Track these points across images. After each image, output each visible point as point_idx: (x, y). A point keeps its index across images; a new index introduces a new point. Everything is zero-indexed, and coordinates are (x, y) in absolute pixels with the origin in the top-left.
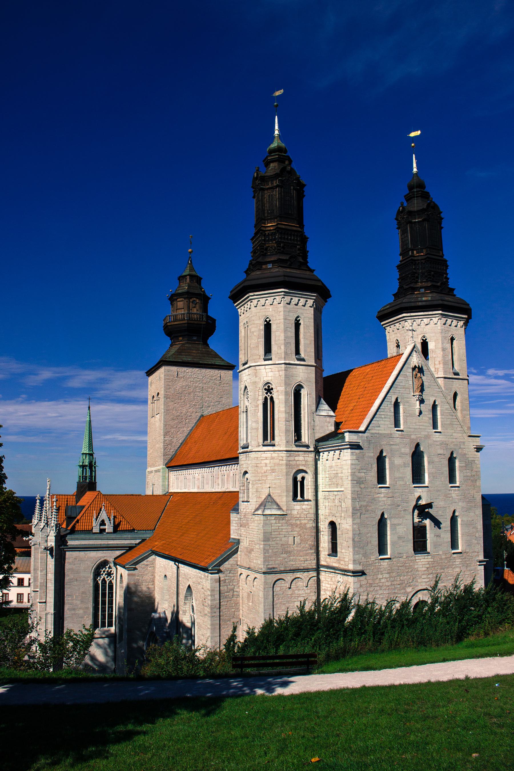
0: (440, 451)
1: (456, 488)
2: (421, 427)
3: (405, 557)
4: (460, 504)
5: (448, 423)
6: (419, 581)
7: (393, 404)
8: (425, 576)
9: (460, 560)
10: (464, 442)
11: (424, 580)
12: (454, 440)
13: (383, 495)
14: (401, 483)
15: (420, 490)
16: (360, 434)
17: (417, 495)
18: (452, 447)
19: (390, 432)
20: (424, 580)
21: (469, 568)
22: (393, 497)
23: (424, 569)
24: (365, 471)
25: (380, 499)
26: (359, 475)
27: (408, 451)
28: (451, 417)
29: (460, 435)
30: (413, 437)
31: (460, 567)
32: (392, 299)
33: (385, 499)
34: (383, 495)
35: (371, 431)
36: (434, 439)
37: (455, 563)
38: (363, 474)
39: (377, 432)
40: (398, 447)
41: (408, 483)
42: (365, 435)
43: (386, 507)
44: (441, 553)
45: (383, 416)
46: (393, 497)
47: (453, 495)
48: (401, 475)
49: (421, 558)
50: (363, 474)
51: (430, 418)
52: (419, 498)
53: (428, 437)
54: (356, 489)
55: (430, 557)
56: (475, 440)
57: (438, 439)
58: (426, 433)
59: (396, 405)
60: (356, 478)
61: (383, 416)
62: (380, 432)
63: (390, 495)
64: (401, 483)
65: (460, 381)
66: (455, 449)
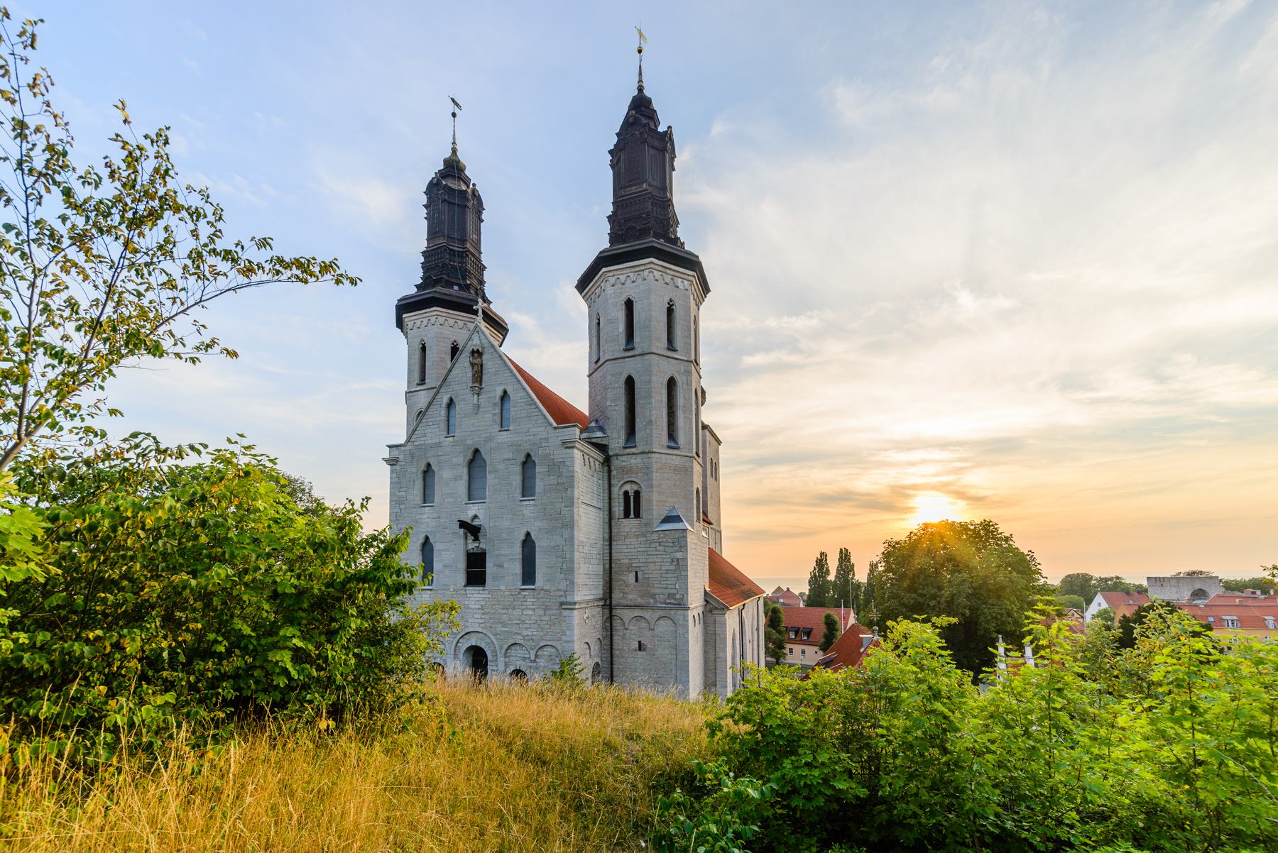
0: (510, 456)
1: (531, 502)
2: (480, 428)
3: (452, 590)
4: (537, 523)
5: (524, 415)
6: (470, 620)
7: (444, 405)
8: (479, 616)
9: (533, 600)
10: (547, 438)
11: (476, 621)
13: (426, 516)
14: (451, 500)
16: (402, 448)
18: (526, 448)
19: (438, 441)
20: (476, 621)
21: (548, 612)
22: (439, 517)
23: (477, 607)
24: (405, 489)
25: (423, 521)
26: (398, 494)
27: (462, 460)
28: (528, 407)
29: (542, 429)
30: (470, 442)
31: (534, 610)
32: (414, 291)
33: (427, 520)
34: (426, 516)
35: (415, 444)
36: (499, 441)
37: (525, 603)
38: (404, 493)
39: (422, 443)
40: (448, 457)
41: (459, 500)
42: (407, 448)
43: (429, 530)
44: (503, 587)
45: (431, 423)
46: (439, 517)
47: (525, 512)
48: (450, 491)
49: (473, 592)
50: (404, 493)
51: (494, 415)
52: (476, 516)
53: (489, 439)
54: (395, 511)
55: (486, 592)
56: (567, 433)
57: (505, 440)
58: (488, 435)
60: (396, 499)
61: (431, 423)
62: (426, 442)
63: (436, 515)
64: (451, 500)
65: (638, 358)
66: (532, 450)
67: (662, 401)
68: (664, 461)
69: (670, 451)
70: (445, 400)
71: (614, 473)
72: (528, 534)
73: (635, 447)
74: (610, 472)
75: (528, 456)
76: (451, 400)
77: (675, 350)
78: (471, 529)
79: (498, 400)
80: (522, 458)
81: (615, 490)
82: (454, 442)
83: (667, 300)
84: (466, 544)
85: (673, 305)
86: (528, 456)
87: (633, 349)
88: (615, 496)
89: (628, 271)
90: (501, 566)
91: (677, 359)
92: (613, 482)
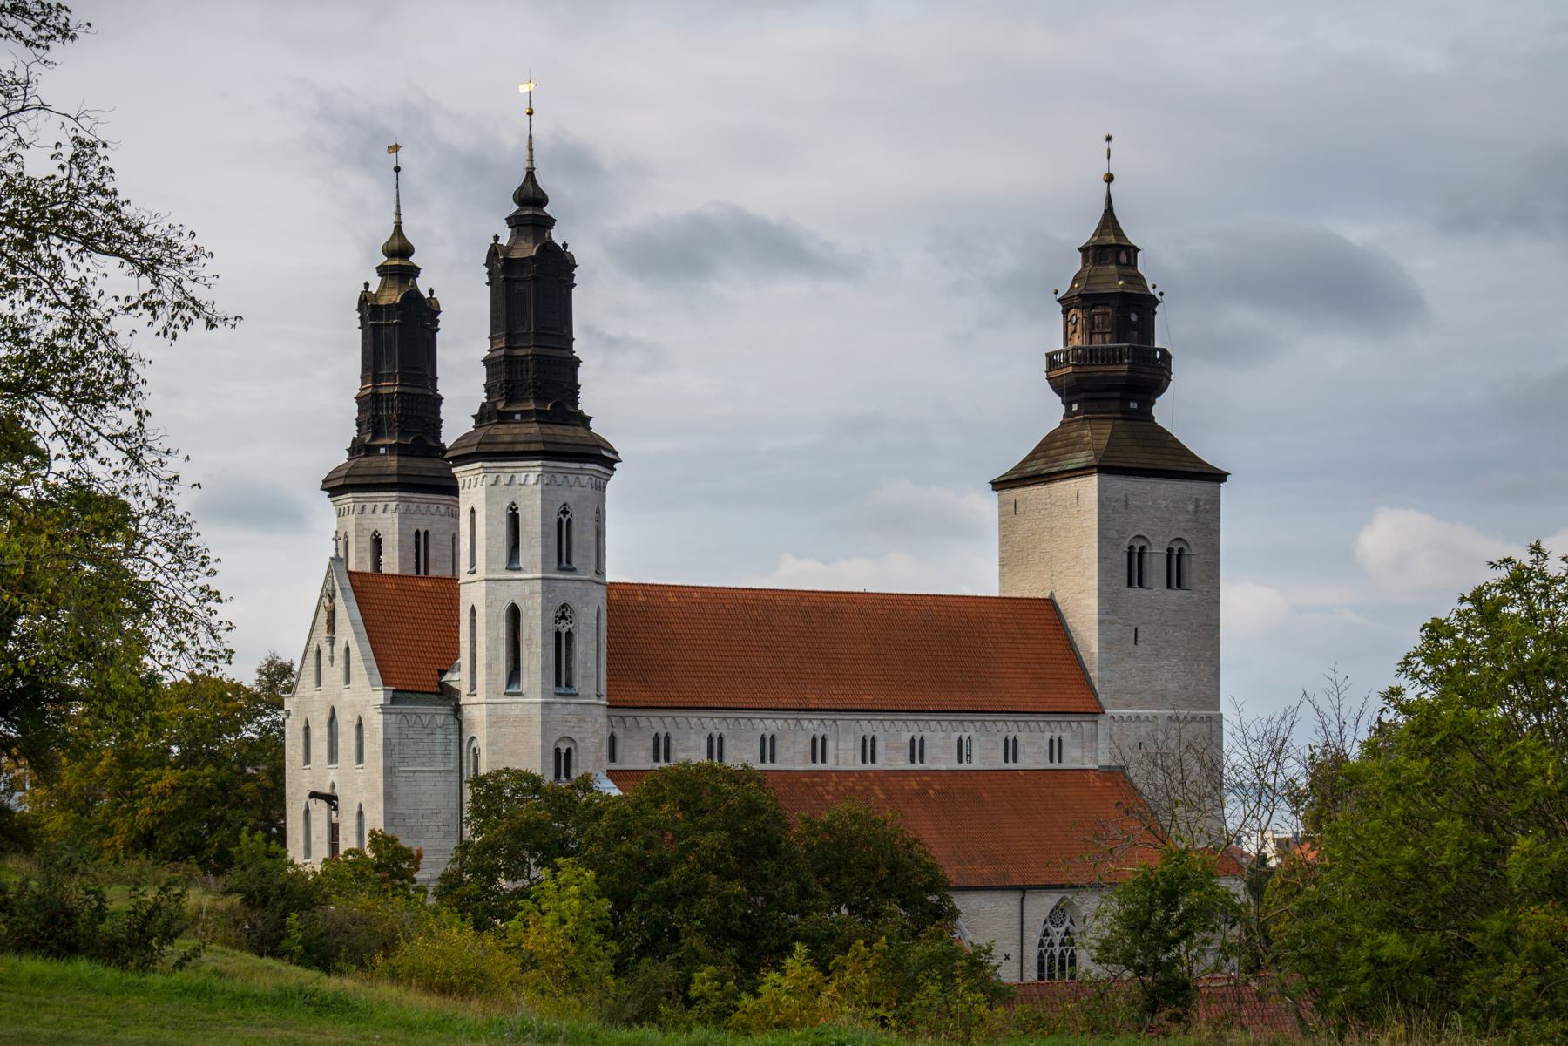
0: (349, 717)
12: (361, 698)
15: (332, 772)
17: (330, 779)
30: (329, 698)
59: (319, 653)
67: (498, 637)
68: (500, 712)
69: (510, 699)
70: (315, 648)
71: (464, 725)
72: (360, 806)
73: (475, 695)
74: (460, 723)
75: (360, 719)
76: (318, 646)
77: (519, 569)
78: (331, 800)
79: (342, 652)
80: (356, 722)
81: (465, 746)
82: (321, 696)
83: (506, 504)
84: (330, 816)
85: (517, 509)
86: (360, 719)
87: (474, 572)
88: (465, 755)
89: (469, 473)
90: (346, 839)
91: (521, 580)
92: (464, 737)
